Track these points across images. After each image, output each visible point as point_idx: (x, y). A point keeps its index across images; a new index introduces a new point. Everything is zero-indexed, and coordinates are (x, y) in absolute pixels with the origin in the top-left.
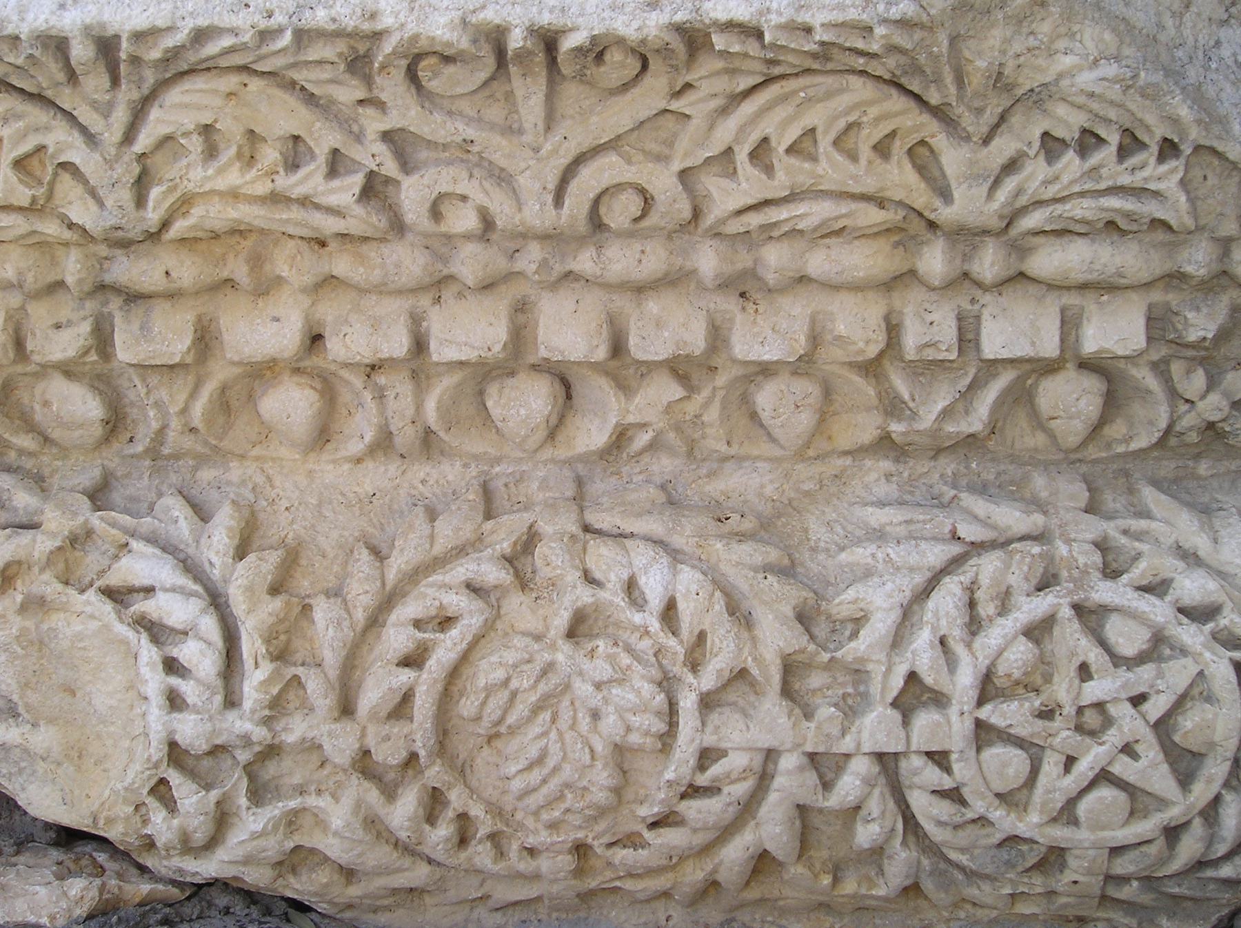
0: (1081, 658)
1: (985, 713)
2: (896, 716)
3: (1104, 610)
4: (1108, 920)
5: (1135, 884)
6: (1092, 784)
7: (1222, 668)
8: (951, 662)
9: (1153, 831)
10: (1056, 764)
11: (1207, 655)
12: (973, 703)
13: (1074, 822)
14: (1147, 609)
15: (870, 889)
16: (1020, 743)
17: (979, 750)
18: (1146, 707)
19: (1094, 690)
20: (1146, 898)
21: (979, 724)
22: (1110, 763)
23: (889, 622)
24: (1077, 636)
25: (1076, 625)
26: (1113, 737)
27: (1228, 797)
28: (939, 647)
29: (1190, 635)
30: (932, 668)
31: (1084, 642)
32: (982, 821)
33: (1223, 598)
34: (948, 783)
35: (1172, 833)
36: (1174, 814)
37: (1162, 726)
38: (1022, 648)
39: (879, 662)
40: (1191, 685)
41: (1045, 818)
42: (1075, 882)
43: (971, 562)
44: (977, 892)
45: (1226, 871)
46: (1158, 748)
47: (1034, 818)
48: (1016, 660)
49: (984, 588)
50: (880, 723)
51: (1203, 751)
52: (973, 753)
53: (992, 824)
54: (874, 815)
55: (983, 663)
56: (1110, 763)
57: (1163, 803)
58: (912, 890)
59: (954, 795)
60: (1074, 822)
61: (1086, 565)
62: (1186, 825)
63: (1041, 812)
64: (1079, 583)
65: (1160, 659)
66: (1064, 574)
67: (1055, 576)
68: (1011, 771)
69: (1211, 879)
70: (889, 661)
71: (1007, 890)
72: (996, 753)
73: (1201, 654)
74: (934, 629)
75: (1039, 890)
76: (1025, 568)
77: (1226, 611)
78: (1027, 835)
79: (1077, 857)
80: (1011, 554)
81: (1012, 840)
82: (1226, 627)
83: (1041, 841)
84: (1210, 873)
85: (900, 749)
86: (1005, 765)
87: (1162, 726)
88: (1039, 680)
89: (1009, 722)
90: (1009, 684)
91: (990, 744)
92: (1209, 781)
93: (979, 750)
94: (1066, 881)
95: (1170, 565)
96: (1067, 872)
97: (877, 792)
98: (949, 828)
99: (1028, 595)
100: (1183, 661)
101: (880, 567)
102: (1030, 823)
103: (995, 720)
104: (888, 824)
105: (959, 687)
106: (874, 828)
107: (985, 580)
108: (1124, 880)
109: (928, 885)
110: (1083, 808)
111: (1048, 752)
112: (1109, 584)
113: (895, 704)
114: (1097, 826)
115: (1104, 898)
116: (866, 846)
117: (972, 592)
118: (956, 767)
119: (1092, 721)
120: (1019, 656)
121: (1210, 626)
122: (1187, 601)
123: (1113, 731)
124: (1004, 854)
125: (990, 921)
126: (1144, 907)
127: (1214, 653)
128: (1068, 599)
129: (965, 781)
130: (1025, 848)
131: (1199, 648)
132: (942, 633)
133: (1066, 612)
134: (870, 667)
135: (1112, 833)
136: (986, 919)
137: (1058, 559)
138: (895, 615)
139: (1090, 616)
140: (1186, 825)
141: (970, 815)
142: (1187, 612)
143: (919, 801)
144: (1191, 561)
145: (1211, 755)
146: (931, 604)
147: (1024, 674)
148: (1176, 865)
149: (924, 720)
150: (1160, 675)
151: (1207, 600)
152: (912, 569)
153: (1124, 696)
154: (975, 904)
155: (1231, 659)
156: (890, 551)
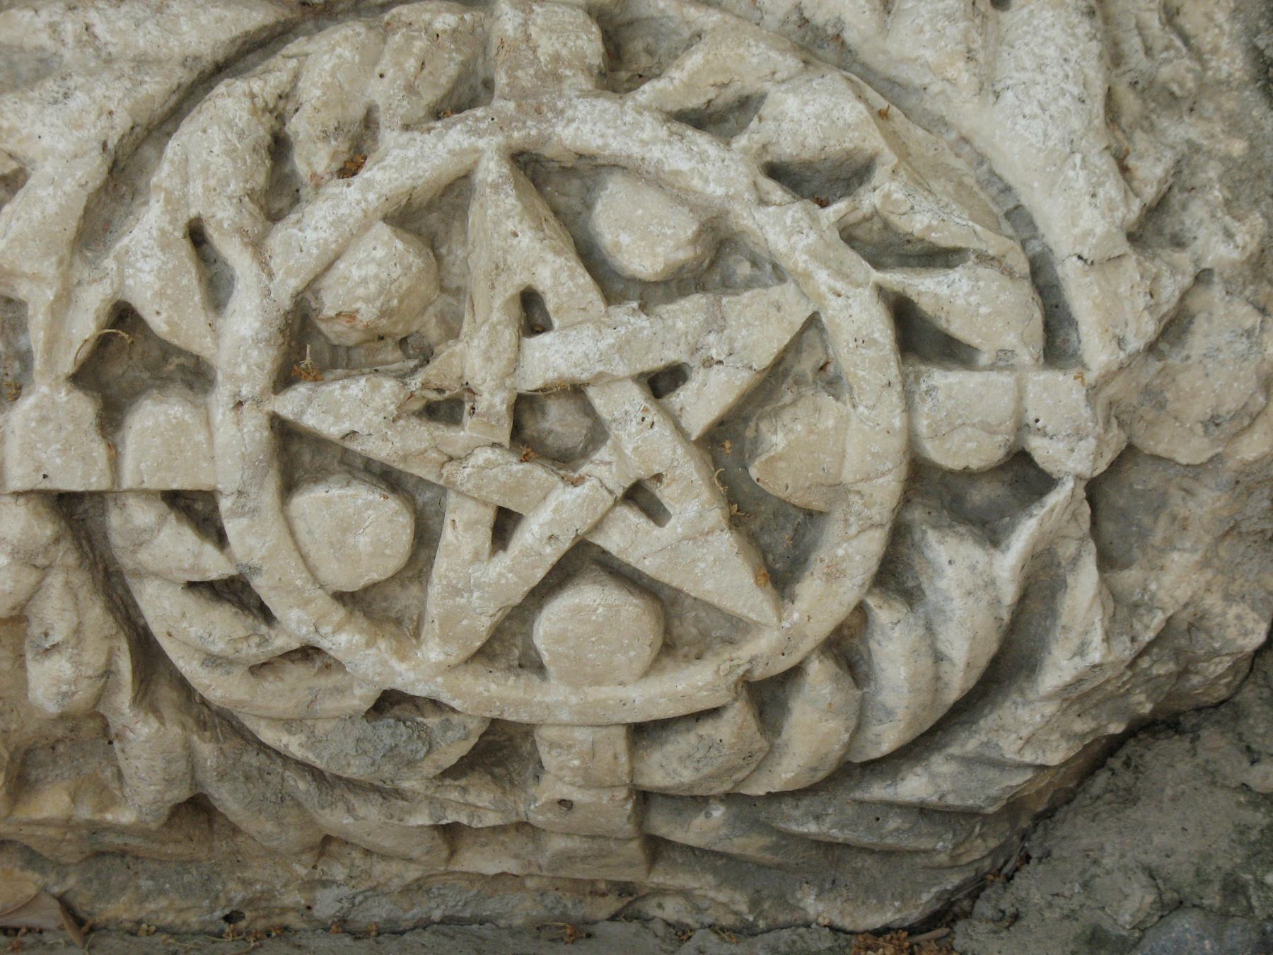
0: (519, 280)
1: (289, 404)
2: (85, 407)
3: (589, 170)
4: (684, 893)
5: (718, 812)
6: (561, 575)
7: (856, 309)
8: (216, 287)
9: (714, 689)
10: (470, 526)
11: (823, 277)
12: (262, 380)
13: (532, 665)
14: (684, 166)
15: (103, 809)
16: (389, 479)
17: (289, 487)
18: (682, 397)
19: (549, 359)
20: (750, 845)
21: (285, 433)
22: (597, 526)
23: (69, 186)
24: (510, 225)
25: (510, 200)
26: (605, 472)
27: (885, 614)
28: (184, 249)
29: (784, 228)
30: (161, 294)
31: (527, 240)
32: (307, 652)
33: (874, 141)
34: (215, 566)
35: (768, 695)
36: (762, 650)
37: (724, 443)
38: (380, 253)
39: (35, 278)
40: (795, 346)
41: (457, 653)
42: (565, 804)
43: (292, 48)
44: (348, 820)
45: (914, 786)
46: (706, 494)
47: (433, 652)
48: (364, 281)
49: (307, 110)
50: (44, 420)
51: (817, 505)
52: (268, 495)
53: (340, 666)
54: (56, 637)
55: (287, 287)
56: (597, 526)
57: (737, 628)
58: (196, 809)
59: (233, 591)
60: (532, 665)
61: (556, 58)
62: (795, 673)
63: (445, 639)
64: (533, 103)
65: (728, 285)
66: (501, 79)
67: (488, 84)
68: (363, 541)
69: (890, 805)
70: (65, 277)
71: (422, 819)
72: (325, 503)
73: (808, 276)
74: (173, 204)
75: (492, 819)
76: (411, 64)
77: (880, 175)
78: (420, 690)
79: (552, 745)
80: (388, 29)
81: (389, 702)
82: (876, 213)
83: (455, 704)
84: (878, 791)
85: (97, 481)
86: (347, 527)
87: (724, 443)
88: (433, 332)
89: (346, 426)
90: (354, 338)
91: (319, 475)
92: (834, 574)
93: (289, 487)
94: (543, 798)
95: (751, 60)
96: (547, 780)
97: (56, 581)
98: (239, 672)
99: (407, 127)
100: (776, 292)
101: (68, 55)
102: (421, 668)
103: (311, 420)
104: (94, 658)
105: (227, 342)
106: (60, 666)
107: (311, 92)
108: (690, 801)
109: (227, 799)
110: (549, 625)
111: (452, 499)
112: (605, 105)
113: (86, 376)
114: (582, 676)
115: (656, 848)
116: (53, 709)
117: (281, 118)
118: (232, 528)
119: (541, 428)
120: (372, 269)
121: (839, 207)
122: (786, 150)
123: (603, 453)
124: (386, 732)
125: (406, 890)
126: (760, 866)
127: (840, 274)
128: (499, 139)
129: (256, 561)
130: (432, 721)
131: (800, 260)
132: (193, 212)
133: (492, 169)
134: (23, 290)
135: (621, 692)
136: (396, 884)
137: (495, 41)
138: (92, 169)
139: (554, 183)
140: (795, 673)
141: (281, 642)
142: (783, 174)
143: (160, 606)
144: (830, 52)
145: (838, 514)
146: (173, 147)
147: (384, 313)
148: (787, 771)
149: (154, 420)
150: (715, 323)
151: (835, 147)
152: (141, 62)
153: (621, 369)
154: (368, 852)
155: (880, 290)
156: (93, 17)
